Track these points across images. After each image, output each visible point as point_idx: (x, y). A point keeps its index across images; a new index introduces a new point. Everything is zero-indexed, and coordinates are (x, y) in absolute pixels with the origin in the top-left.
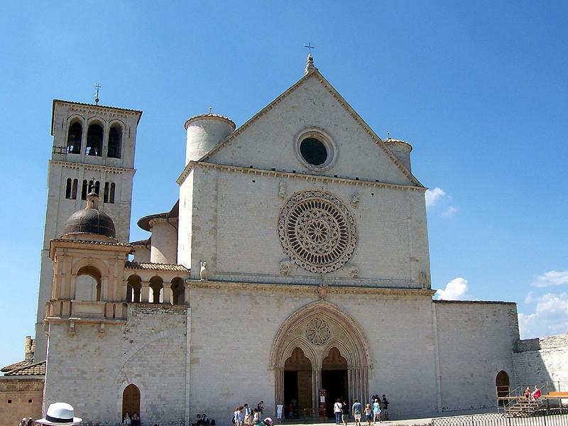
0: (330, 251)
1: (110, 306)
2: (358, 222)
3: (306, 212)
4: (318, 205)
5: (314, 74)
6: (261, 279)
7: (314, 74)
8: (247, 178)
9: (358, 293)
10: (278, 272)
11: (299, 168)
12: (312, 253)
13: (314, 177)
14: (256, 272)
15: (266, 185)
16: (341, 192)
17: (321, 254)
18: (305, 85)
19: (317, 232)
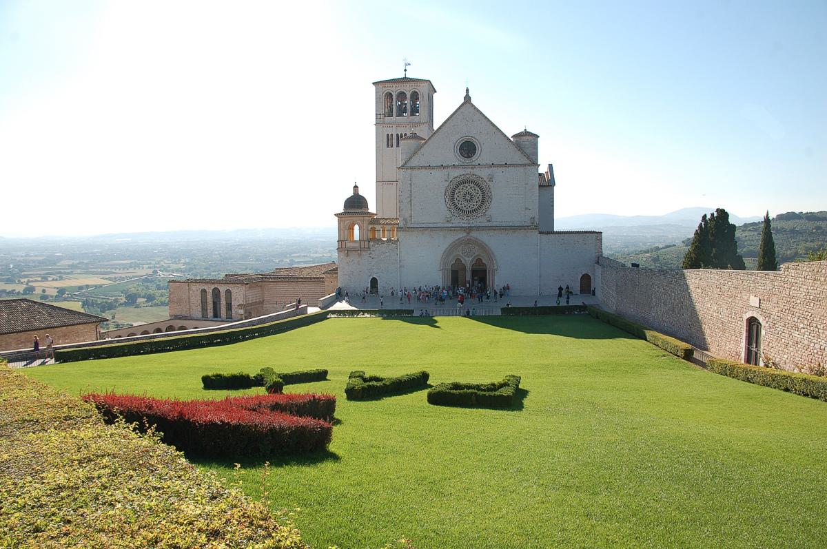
0: (475, 207)
1: (362, 243)
2: (492, 189)
3: (461, 187)
4: (468, 181)
5: (467, 99)
6: (435, 225)
7: (467, 99)
8: (428, 171)
9: (489, 230)
10: (444, 221)
11: (457, 164)
12: (464, 209)
13: (465, 167)
14: (432, 221)
15: (439, 175)
16: (483, 173)
17: (470, 209)
18: (461, 110)
19: (469, 197)
